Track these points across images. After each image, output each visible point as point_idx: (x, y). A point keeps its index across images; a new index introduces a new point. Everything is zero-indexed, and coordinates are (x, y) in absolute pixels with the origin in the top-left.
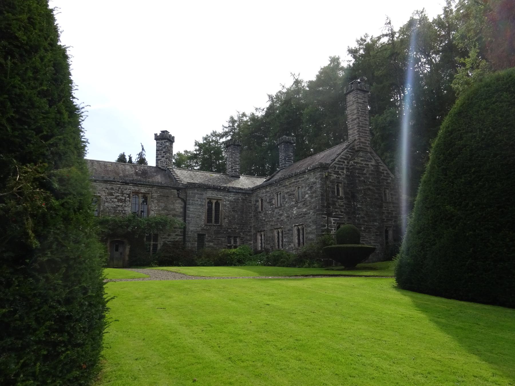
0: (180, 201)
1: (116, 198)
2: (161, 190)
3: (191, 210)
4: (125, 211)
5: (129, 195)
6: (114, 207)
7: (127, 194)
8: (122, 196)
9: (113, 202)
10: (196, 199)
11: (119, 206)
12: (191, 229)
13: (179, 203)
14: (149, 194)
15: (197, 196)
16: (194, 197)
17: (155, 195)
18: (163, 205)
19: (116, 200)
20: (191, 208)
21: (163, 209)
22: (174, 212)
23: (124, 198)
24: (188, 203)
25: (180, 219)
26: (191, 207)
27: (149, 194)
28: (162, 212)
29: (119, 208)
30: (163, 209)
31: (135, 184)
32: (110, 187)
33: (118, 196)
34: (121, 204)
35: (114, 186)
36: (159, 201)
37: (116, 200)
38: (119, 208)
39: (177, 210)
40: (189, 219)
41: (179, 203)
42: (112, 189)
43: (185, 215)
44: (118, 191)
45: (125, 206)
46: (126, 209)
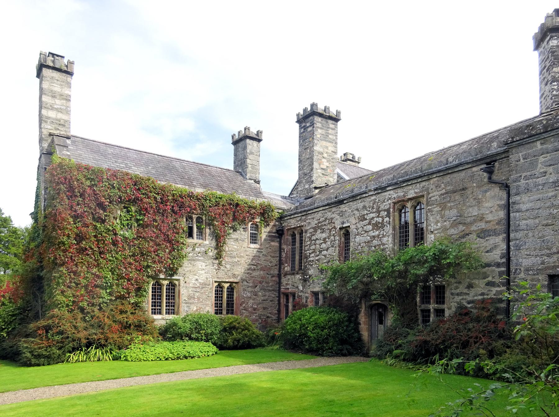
0: (496, 191)
1: (369, 224)
2: (447, 178)
3: (523, 207)
4: (384, 244)
5: (388, 211)
6: (368, 242)
7: (385, 210)
8: (378, 217)
9: (366, 232)
10: (540, 168)
11: (374, 237)
12: (526, 262)
13: (493, 197)
14: (423, 196)
15: (541, 159)
16: (533, 165)
17: (435, 195)
18: (454, 212)
19: (370, 227)
20: (524, 202)
21: (455, 224)
22: (483, 225)
23: (380, 220)
24: (513, 191)
25: (499, 240)
26: (524, 198)
27: (423, 196)
28: (452, 231)
29: (375, 242)
30: (455, 224)
31: (396, 184)
32: (362, 204)
33: (373, 218)
34: (377, 233)
35: (368, 202)
36: (443, 207)
37: (370, 227)
38: (375, 242)
39: (490, 217)
40: (519, 235)
41: (493, 197)
42: (364, 207)
43: (508, 226)
44: (373, 208)
45: (384, 236)
46: (385, 240)
